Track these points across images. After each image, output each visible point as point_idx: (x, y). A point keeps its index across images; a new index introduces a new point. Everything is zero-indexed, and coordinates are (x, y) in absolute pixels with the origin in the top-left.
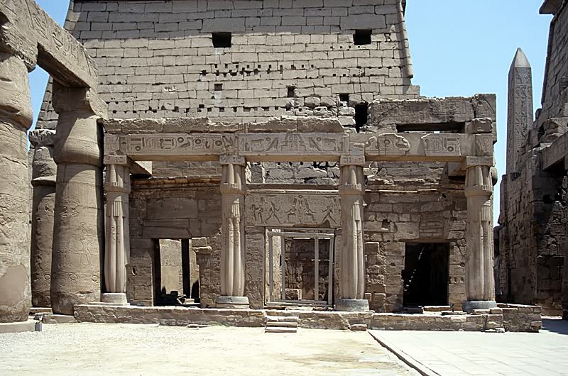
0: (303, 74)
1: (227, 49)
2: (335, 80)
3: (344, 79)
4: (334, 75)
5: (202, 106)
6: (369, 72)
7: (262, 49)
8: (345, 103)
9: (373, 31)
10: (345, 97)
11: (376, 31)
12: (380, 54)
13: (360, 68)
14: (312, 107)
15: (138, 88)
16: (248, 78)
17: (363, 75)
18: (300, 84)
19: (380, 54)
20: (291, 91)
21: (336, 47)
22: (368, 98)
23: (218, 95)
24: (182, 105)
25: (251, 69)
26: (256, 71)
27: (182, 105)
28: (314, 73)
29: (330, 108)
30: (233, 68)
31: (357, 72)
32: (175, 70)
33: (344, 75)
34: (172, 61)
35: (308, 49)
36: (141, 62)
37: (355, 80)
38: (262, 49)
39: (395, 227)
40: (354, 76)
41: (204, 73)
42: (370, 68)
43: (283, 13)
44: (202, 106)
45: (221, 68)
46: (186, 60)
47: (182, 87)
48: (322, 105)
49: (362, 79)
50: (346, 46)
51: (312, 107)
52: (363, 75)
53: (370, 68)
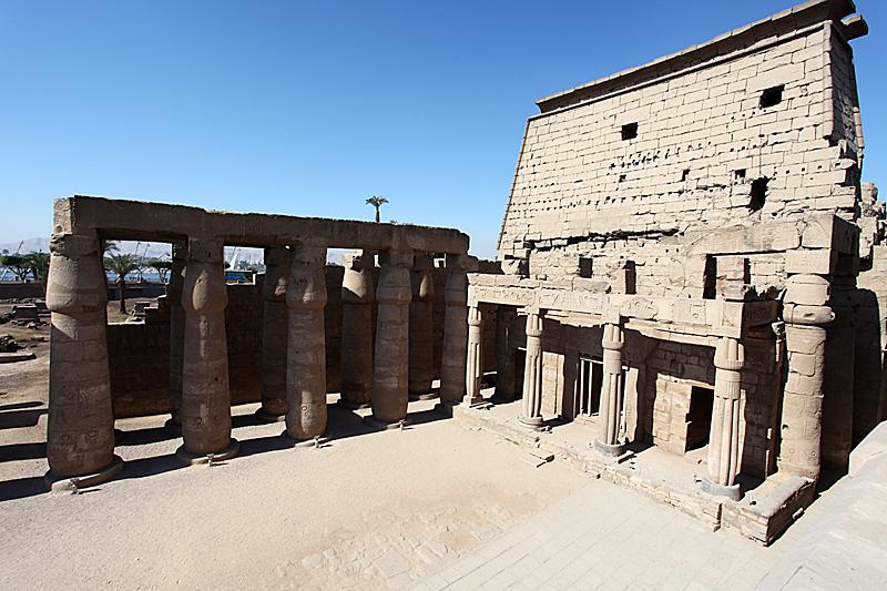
0: (699, 154)
1: (633, 140)
4: (732, 150)
5: (608, 198)
7: (665, 133)
8: (739, 180)
9: (786, 87)
10: (742, 173)
11: (791, 85)
12: (791, 113)
13: (763, 136)
14: (706, 188)
15: (564, 187)
16: (648, 166)
18: (695, 165)
19: (791, 113)
20: (686, 172)
23: (624, 184)
24: (594, 198)
25: (651, 156)
26: (655, 157)
27: (594, 198)
29: (724, 187)
30: (635, 157)
32: (592, 166)
33: (743, 148)
34: (588, 159)
35: (708, 125)
36: (568, 164)
37: (756, 151)
38: (665, 133)
39: (683, 368)
40: (755, 146)
41: (613, 166)
42: (775, 134)
43: (687, 90)
44: (608, 198)
45: (627, 160)
46: (600, 157)
47: (596, 182)
48: (718, 186)
49: (766, 149)
51: (706, 188)
53: (775, 134)
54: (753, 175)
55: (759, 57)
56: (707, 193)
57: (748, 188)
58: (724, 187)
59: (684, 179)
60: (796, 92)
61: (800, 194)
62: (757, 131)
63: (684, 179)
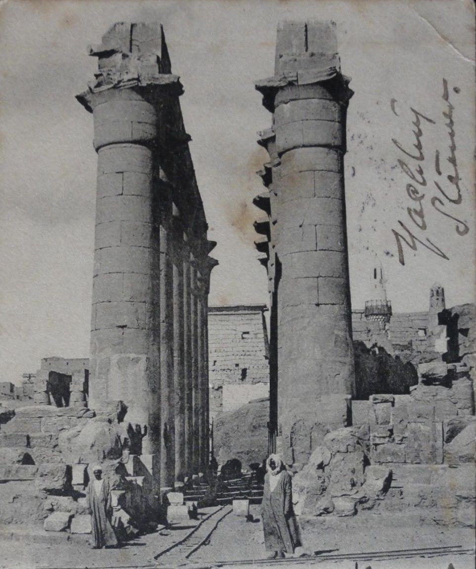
0: (220, 354)
2: (233, 357)
3: (238, 357)
6: (248, 353)
10: (237, 365)
12: (252, 344)
14: (224, 370)
17: (245, 355)
21: (234, 341)
22: (247, 366)
28: (224, 354)
29: (231, 370)
31: (243, 353)
37: (242, 357)
49: (245, 357)
50: (238, 341)
51: (224, 370)
52: (245, 355)
54: (242, 366)
55: (240, 318)
56: (225, 372)
57: (240, 372)
58: (231, 370)
59: (214, 365)
60: (253, 336)
61: (258, 376)
62: (242, 348)
63: (214, 365)
